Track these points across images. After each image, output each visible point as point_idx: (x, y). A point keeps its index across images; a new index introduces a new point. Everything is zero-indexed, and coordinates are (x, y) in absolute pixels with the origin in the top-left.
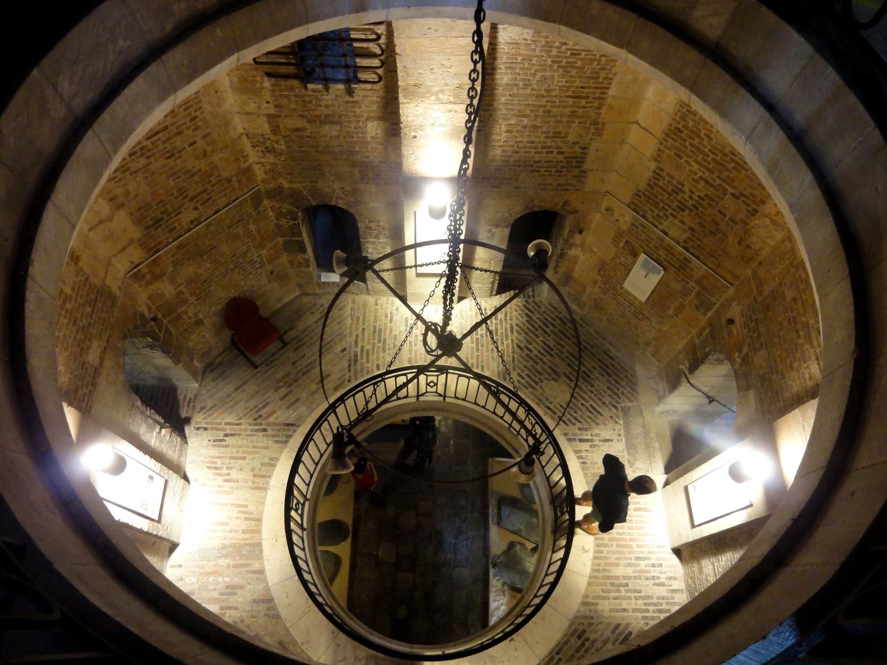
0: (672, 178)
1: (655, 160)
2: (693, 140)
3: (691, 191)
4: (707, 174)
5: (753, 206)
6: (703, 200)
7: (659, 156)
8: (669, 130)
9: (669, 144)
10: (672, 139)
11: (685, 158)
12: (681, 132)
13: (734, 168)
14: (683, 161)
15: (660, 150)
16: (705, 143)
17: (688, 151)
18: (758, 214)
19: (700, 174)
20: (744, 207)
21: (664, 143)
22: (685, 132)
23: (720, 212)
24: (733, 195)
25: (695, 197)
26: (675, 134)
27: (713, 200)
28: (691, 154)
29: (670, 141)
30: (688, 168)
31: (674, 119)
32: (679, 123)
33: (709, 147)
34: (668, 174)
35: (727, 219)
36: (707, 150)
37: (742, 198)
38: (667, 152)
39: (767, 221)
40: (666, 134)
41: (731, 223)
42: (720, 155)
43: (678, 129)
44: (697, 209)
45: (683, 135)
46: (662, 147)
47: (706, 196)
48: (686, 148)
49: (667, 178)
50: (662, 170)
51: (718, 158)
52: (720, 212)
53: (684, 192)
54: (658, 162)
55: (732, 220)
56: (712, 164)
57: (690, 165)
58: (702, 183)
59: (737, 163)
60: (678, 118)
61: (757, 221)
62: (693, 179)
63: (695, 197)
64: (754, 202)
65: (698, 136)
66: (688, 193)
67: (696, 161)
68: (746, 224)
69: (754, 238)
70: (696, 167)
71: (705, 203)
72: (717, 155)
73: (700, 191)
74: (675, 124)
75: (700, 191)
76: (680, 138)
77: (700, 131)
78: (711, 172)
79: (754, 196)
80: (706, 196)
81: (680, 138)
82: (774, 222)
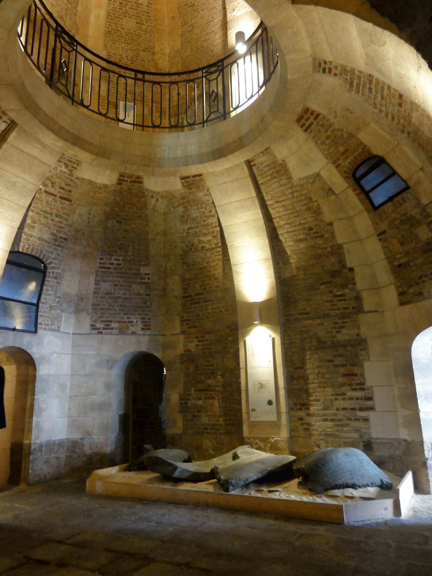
0: (116, 55)
1: (105, 50)
2: (117, 33)
3: (127, 57)
4: (129, 46)
5: (152, 51)
6: (133, 58)
7: (106, 47)
8: (106, 33)
9: (108, 40)
10: (108, 36)
11: (117, 43)
12: (111, 32)
13: (137, 38)
14: (117, 45)
15: (105, 44)
16: (122, 32)
17: (117, 39)
18: (155, 54)
19: (126, 47)
20: (149, 53)
21: (106, 40)
22: (112, 31)
23: (142, 60)
24: (143, 51)
25: (129, 58)
26: (109, 34)
27: (137, 56)
28: (119, 40)
29: (108, 38)
30: (120, 47)
31: (106, 27)
32: (108, 28)
33: (124, 34)
34: (114, 54)
35: (146, 62)
36: (124, 36)
37: (146, 50)
38: (109, 44)
39: (160, 55)
40: (105, 36)
41: (149, 63)
42: (130, 35)
43: (109, 31)
44: (133, 64)
45: (112, 33)
46: (105, 42)
47: (133, 56)
48: (116, 38)
49: (114, 56)
50: (110, 53)
51: (130, 37)
52: (142, 60)
53: (124, 59)
54: (107, 50)
55: (148, 61)
56: (129, 41)
57: (121, 45)
58: (129, 51)
59: (137, 35)
60: (108, 26)
61: (157, 57)
62: (125, 51)
63: (129, 58)
64: (151, 49)
65: (119, 30)
66: (126, 58)
67: (122, 42)
68: (154, 60)
69: (160, 65)
70: (123, 45)
71: (135, 59)
72: (129, 36)
73: (130, 55)
74: (107, 30)
75: (130, 55)
76: (112, 35)
77: (118, 27)
78: (130, 44)
79: (150, 47)
80: (133, 56)
81: (112, 35)
82: (162, 54)
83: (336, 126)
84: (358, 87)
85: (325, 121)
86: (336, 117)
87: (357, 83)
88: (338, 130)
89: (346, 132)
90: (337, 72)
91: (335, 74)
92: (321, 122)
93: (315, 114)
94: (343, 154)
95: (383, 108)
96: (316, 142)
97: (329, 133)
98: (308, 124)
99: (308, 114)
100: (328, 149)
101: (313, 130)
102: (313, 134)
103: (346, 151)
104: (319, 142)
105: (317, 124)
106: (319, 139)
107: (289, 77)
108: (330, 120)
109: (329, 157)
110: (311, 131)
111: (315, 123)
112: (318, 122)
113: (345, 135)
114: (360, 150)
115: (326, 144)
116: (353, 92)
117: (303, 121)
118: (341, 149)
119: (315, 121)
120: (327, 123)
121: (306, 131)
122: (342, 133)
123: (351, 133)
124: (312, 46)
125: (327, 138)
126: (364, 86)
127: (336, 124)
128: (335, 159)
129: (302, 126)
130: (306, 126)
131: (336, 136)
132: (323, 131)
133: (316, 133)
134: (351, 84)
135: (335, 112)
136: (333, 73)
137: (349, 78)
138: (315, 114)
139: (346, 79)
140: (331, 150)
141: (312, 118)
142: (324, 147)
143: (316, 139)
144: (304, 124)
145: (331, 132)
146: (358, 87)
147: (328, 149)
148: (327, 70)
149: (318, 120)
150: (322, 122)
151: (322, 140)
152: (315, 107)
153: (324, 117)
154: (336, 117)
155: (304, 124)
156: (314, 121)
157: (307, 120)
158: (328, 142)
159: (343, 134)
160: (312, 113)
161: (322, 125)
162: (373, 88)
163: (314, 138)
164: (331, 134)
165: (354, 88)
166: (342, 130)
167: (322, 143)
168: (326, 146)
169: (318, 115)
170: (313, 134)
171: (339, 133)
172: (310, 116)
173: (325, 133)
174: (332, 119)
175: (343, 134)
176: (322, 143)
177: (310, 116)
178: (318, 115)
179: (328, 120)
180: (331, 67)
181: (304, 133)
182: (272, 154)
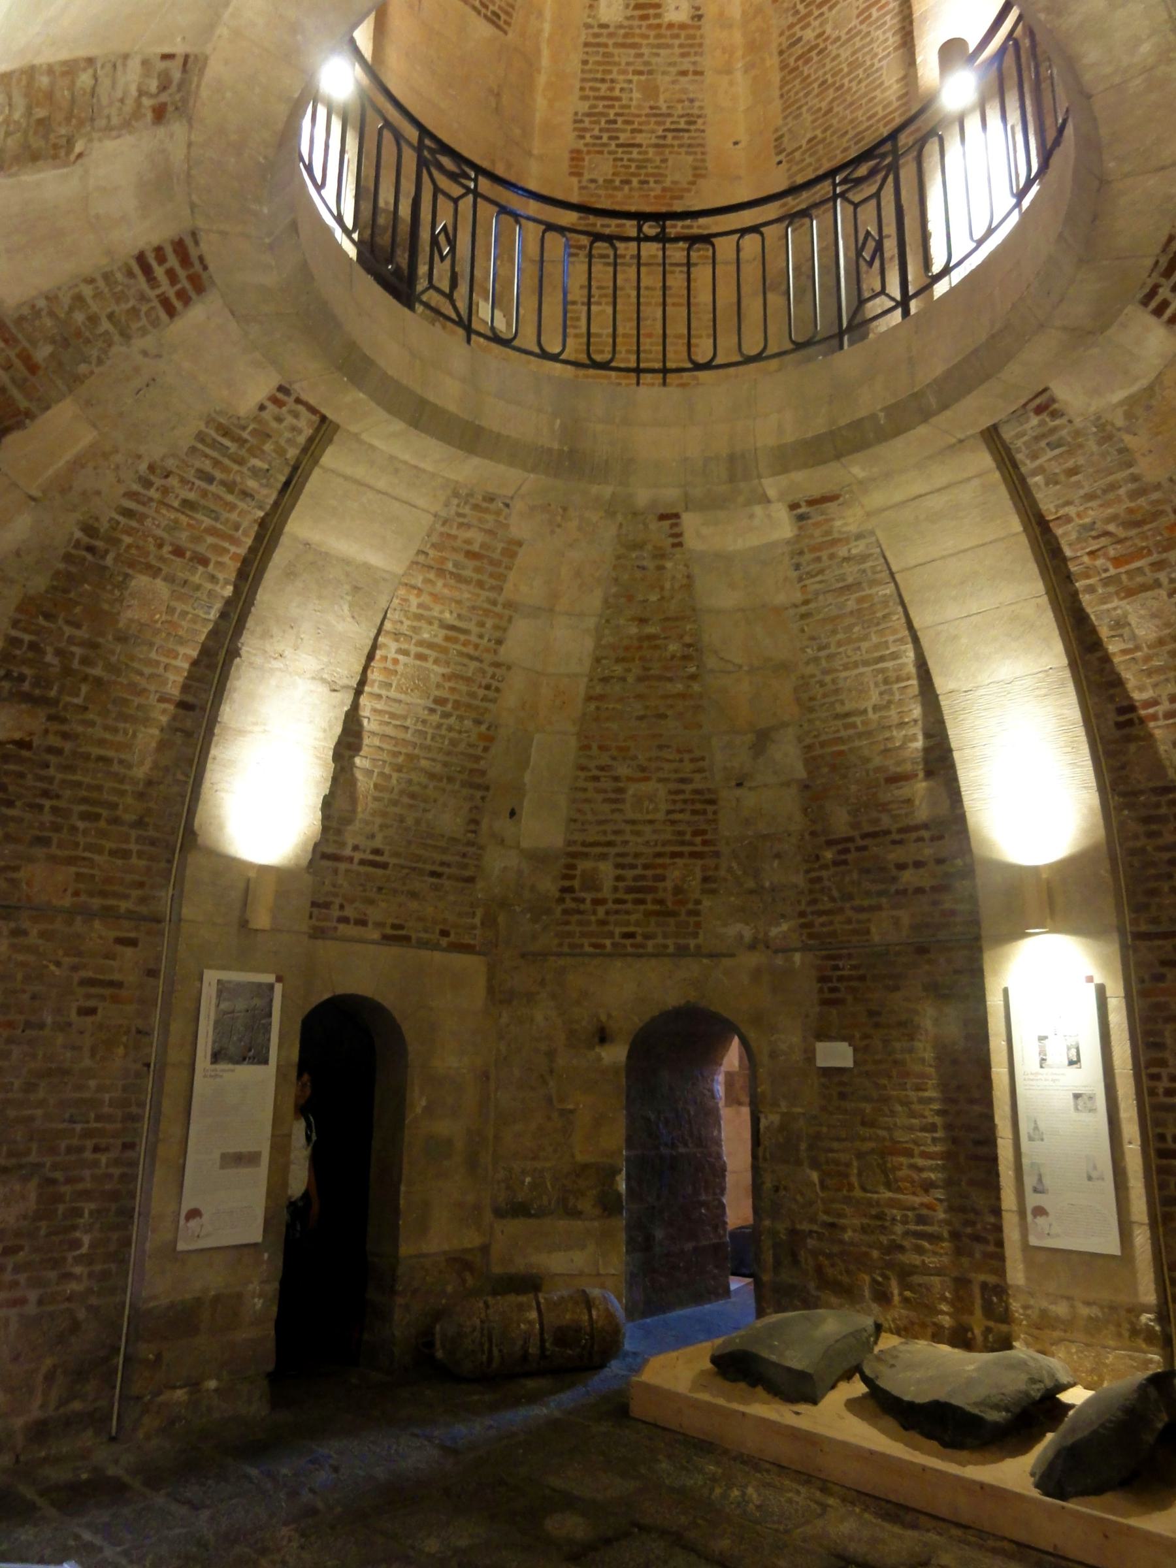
83: (115, 349)
84: (214, 444)
85: (144, 321)
86: (145, 353)
87: (228, 448)
88: (106, 352)
89: (92, 373)
90: (265, 415)
91: (262, 408)
92: (144, 308)
93: (178, 304)
94: (26, 358)
95: (152, 493)
96: (91, 281)
97: (105, 325)
98: (159, 271)
99: (184, 283)
100: (52, 314)
101: (132, 281)
102: (119, 276)
103: (33, 368)
104: (87, 291)
105: (143, 298)
106: (98, 295)
107: (361, 395)
108: (143, 335)
109: (26, 311)
110: (130, 274)
111: (152, 294)
112: (149, 300)
113: (83, 368)
114: (23, 403)
115: (71, 309)
116: (202, 427)
117: (173, 261)
118: (42, 353)
119: (158, 296)
120: (135, 326)
121: (141, 258)
122: (94, 362)
123: (83, 382)
124: (372, 447)
125: (93, 319)
126: (216, 463)
127: (123, 349)
128: (14, 330)
129: (159, 250)
130: (154, 264)
131: (88, 341)
132: (114, 307)
133: (120, 288)
134: (226, 433)
135: (159, 356)
136: (269, 404)
137: (245, 435)
138: (178, 304)
139: (244, 428)
140: (48, 322)
141: (171, 293)
142: (66, 301)
143: (101, 283)
144: (161, 259)
145: (107, 332)
146: (214, 444)
147: (52, 314)
148: (280, 396)
149: (156, 303)
150: (142, 314)
151: (90, 301)
152: (197, 313)
153: (155, 323)
154: (145, 353)
155: (161, 259)
156: (158, 291)
157: (172, 275)
158: (79, 317)
159: (90, 363)
160: (182, 296)
161: (134, 312)
162: (213, 488)
163: (107, 277)
164: (101, 330)
165: (213, 433)
166: (100, 362)
167: (79, 299)
168: (66, 307)
169: (171, 312)
170: (119, 276)
171: (95, 353)
172: (178, 286)
173: (111, 316)
174: (139, 343)
175: (90, 363)
176: (79, 299)
177: (178, 286)
178: (171, 312)
179: (144, 332)
180: (284, 409)
181: (136, 252)
182: (127, 125)
